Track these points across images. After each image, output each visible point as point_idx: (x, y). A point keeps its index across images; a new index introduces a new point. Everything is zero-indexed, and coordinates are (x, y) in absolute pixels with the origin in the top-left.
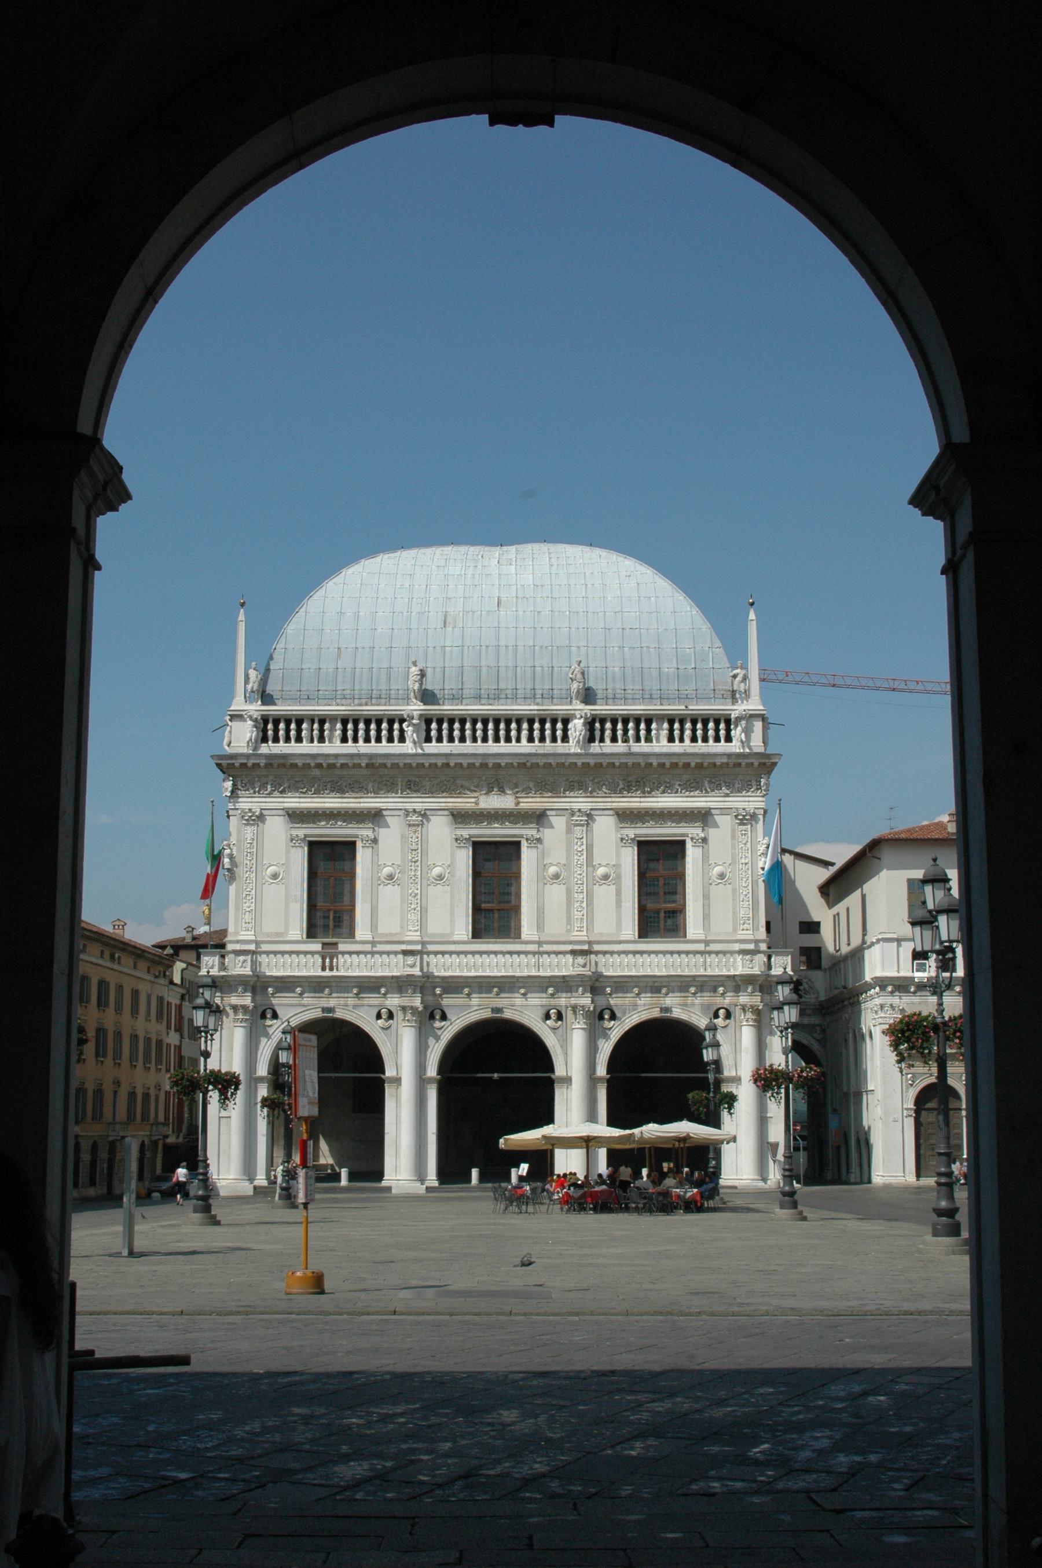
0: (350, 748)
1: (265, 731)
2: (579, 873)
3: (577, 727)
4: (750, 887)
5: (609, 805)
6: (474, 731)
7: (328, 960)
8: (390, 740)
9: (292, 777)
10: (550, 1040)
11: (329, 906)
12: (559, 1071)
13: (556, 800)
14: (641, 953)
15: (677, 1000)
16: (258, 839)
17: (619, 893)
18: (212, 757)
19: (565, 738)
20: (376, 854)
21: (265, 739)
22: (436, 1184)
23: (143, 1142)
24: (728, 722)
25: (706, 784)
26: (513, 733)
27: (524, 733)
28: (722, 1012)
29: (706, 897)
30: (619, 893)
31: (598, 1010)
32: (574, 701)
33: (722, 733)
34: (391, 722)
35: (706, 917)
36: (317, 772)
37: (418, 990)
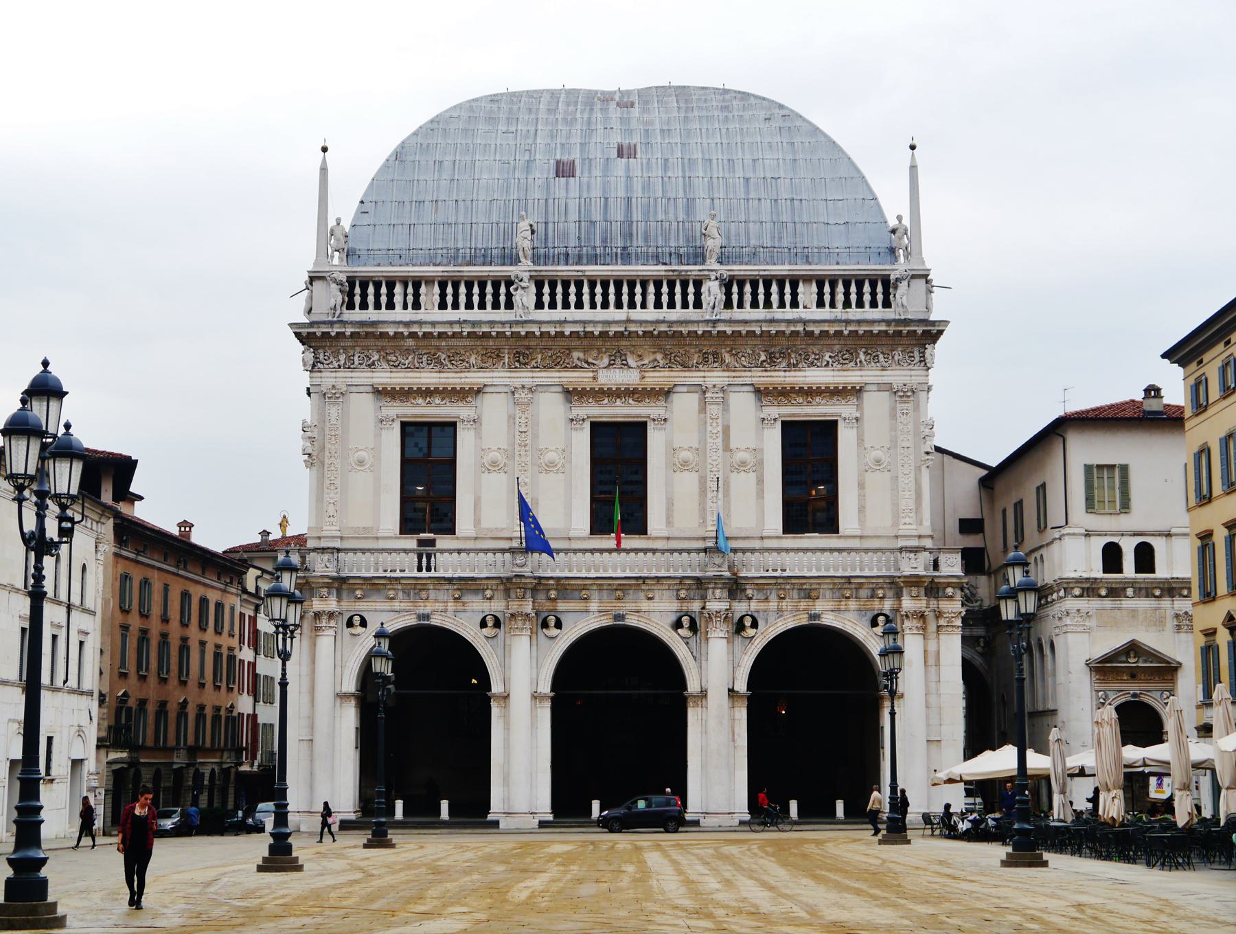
0: (450, 314)
1: (351, 295)
2: (716, 457)
3: (712, 291)
4: (912, 475)
5: (748, 381)
6: (592, 295)
7: (424, 559)
8: (496, 306)
9: (383, 348)
10: (681, 651)
12: (693, 686)
13: (687, 374)
14: (787, 550)
15: (830, 605)
17: (760, 481)
18: (290, 325)
19: (698, 304)
20: (479, 435)
21: (351, 306)
22: (550, 817)
23: (213, 770)
25: (862, 357)
26: (638, 299)
27: (651, 299)
29: (861, 486)
30: (760, 481)
31: (737, 617)
32: (708, 261)
33: (880, 297)
34: (496, 285)
35: (862, 510)
37: (529, 593)
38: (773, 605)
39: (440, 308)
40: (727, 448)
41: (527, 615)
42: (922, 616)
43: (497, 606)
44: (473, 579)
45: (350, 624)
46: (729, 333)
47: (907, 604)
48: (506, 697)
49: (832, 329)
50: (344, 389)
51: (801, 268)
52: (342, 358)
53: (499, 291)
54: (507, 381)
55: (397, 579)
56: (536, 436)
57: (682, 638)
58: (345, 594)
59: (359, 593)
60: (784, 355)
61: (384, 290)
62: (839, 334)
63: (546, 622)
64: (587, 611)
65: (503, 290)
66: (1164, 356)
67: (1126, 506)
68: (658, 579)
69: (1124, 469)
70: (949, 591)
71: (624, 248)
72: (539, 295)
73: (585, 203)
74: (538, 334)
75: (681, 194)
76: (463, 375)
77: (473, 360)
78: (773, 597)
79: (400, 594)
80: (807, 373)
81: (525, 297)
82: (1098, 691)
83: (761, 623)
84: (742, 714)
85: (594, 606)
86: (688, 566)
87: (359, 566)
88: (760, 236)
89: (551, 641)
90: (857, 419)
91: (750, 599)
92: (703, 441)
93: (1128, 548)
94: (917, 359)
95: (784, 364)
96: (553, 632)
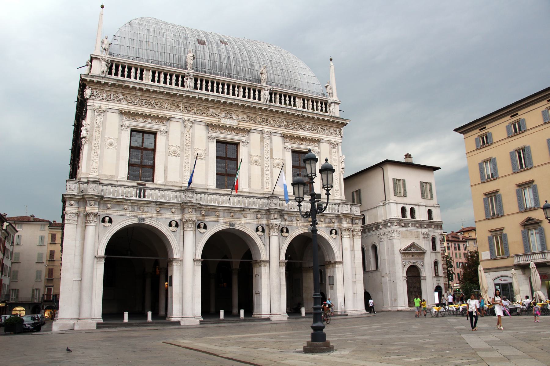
1: (110, 69)
3: (265, 94)
5: (279, 132)
7: (142, 192)
10: (258, 241)
11: (142, 163)
13: (256, 125)
16: (104, 122)
19: (259, 99)
20: (167, 139)
21: (110, 73)
22: (202, 319)
24: (326, 105)
28: (334, 231)
31: (281, 226)
36: (139, 93)
37: (194, 210)
38: (294, 223)
40: (272, 158)
41: (193, 221)
42: (349, 230)
43: (177, 217)
44: (168, 203)
45: (103, 221)
46: (274, 111)
47: (345, 225)
48: (181, 260)
49: (311, 116)
50: (105, 109)
51: (298, 93)
52: (105, 95)
53: (180, 79)
54: (181, 117)
55: (129, 200)
56: (193, 143)
57: (259, 236)
58: (101, 205)
59: (109, 205)
60: (293, 124)
61: (126, 69)
62: (313, 118)
63: (201, 226)
64: (218, 222)
65: (180, 79)
66: (455, 130)
67: (405, 195)
68: (250, 209)
69: (404, 181)
70: (357, 221)
71: (228, 74)
72: (196, 84)
73: (212, 56)
74: (197, 98)
75: (248, 60)
76: (162, 111)
77: (166, 105)
78: (294, 220)
79: (130, 208)
80: (301, 132)
81: (190, 83)
82: (403, 261)
83: (290, 231)
84: (283, 270)
85: (221, 219)
86: (263, 204)
87: (111, 192)
88: (278, 79)
89: (201, 235)
90: (319, 152)
91: (285, 220)
92: (262, 153)
93: (408, 208)
94: (338, 133)
95: (292, 127)
96: (202, 230)
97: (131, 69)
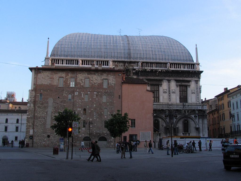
39: (66, 64)
61: (57, 61)
97: (59, 60)
